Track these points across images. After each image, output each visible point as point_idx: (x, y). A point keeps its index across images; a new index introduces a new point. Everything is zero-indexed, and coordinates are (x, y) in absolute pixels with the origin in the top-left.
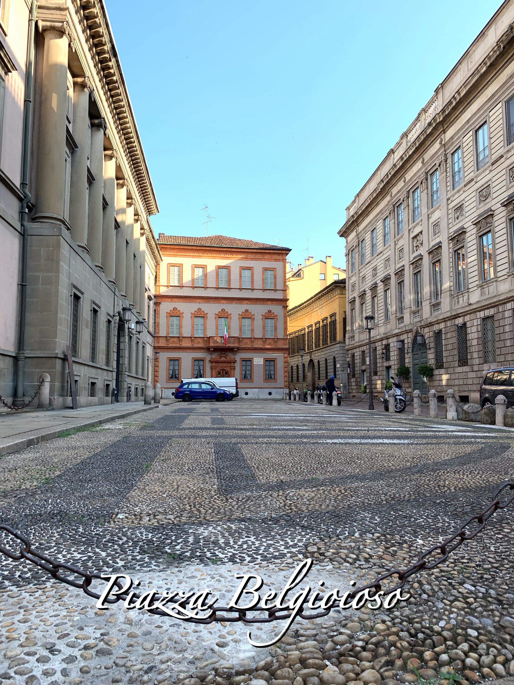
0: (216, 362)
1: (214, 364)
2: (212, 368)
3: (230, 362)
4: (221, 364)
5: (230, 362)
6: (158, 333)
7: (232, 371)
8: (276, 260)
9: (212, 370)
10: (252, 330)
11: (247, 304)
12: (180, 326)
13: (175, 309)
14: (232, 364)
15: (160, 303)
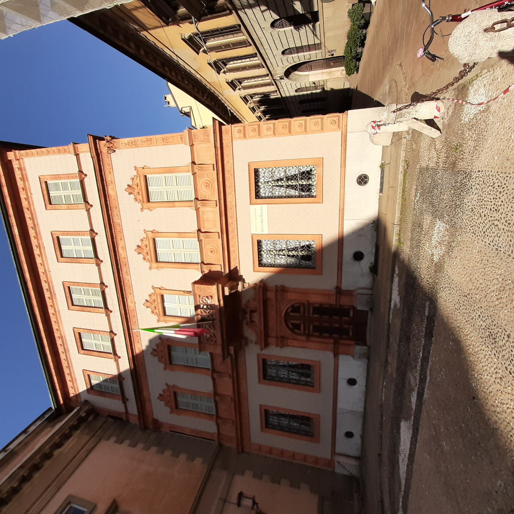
0: (267, 336)
1: (272, 340)
2: (282, 342)
3: (265, 301)
4: (272, 323)
5: (265, 301)
6: (212, 434)
7: (290, 296)
8: (24, 179)
9: (288, 346)
10: (181, 234)
11: (124, 248)
12: (195, 394)
13: (161, 397)
14: (271, 295)
15: (156, 422)
